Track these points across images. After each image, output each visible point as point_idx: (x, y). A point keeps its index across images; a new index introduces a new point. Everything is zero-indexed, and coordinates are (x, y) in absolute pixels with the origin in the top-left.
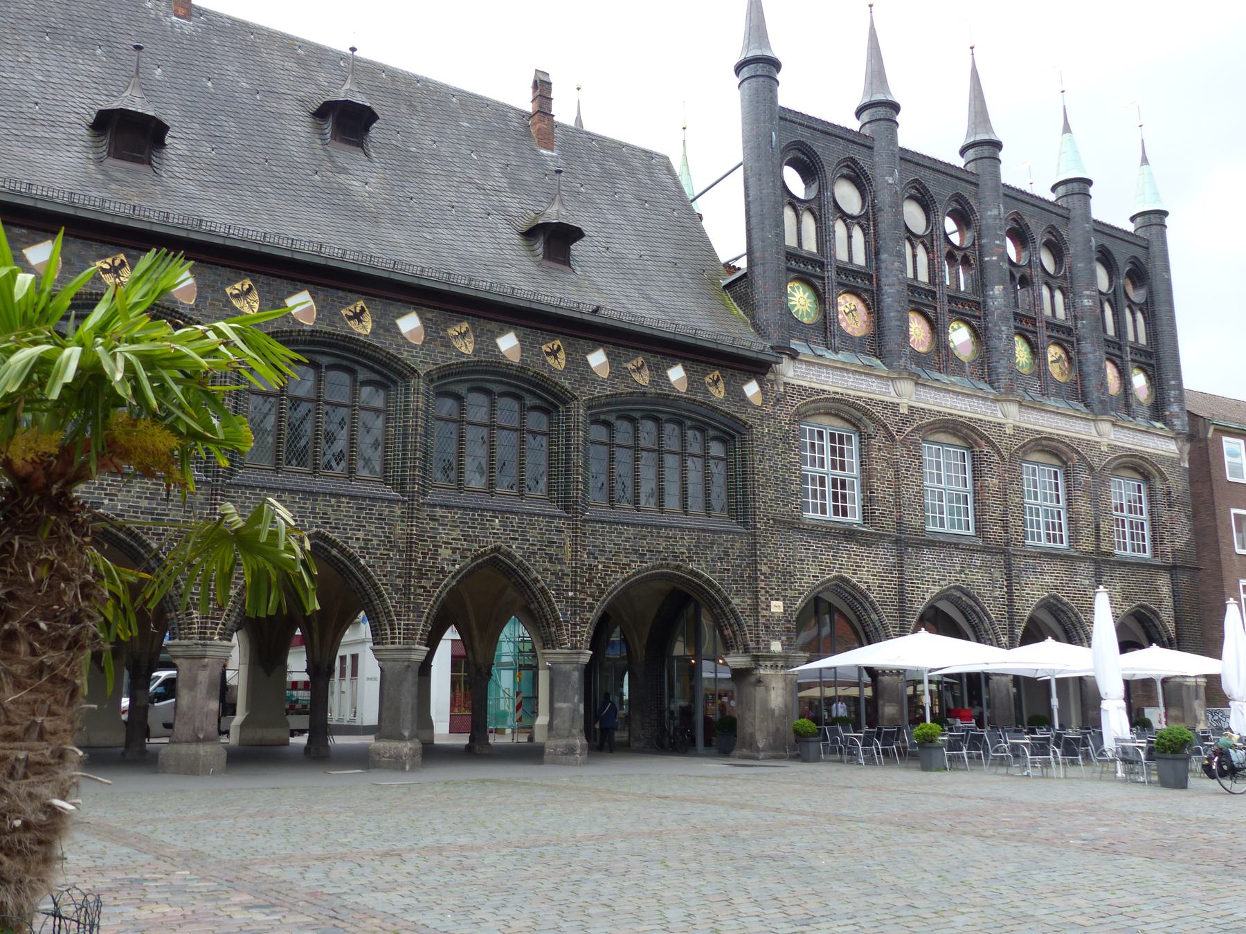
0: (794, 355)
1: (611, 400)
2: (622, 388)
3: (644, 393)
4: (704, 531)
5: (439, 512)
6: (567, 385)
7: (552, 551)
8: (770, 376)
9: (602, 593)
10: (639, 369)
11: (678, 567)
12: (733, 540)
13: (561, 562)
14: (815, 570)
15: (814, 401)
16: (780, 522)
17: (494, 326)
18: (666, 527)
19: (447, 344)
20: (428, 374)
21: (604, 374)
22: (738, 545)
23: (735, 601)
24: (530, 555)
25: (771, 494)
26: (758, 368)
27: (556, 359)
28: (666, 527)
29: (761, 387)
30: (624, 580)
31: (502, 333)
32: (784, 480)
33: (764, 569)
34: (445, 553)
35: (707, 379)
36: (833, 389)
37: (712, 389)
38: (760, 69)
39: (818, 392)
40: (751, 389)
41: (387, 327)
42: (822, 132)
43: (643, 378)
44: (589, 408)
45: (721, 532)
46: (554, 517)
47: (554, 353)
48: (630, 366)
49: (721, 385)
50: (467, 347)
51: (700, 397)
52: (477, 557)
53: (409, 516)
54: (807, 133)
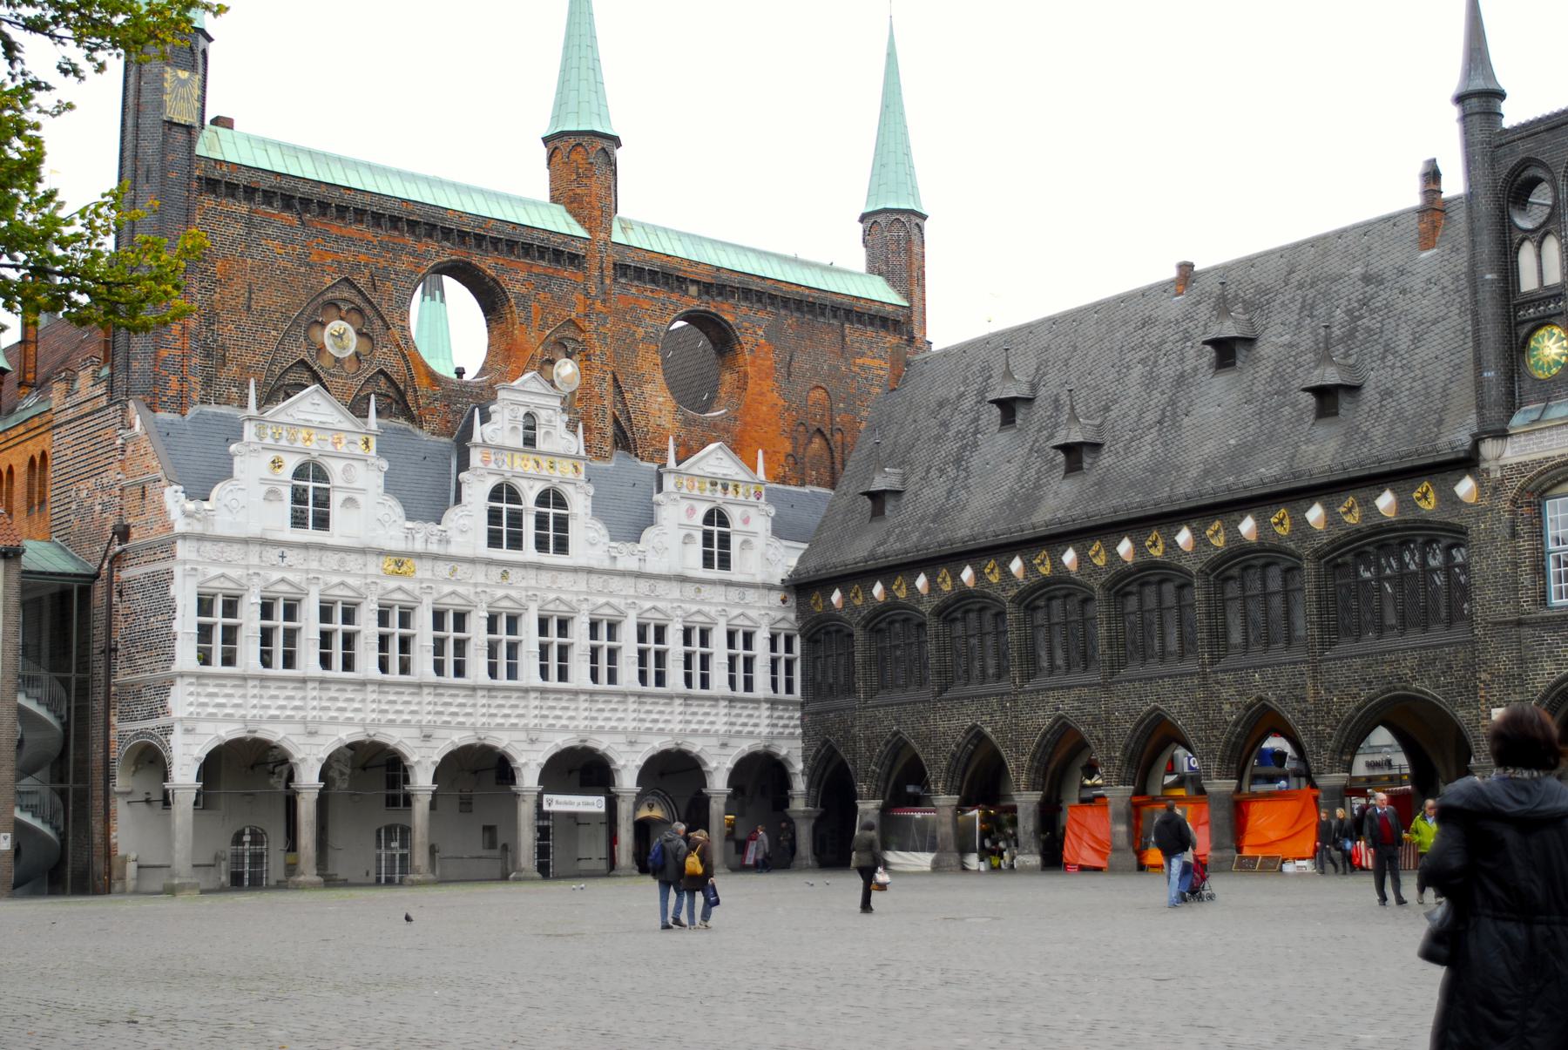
0: (1502, 434)
1: (1336, 546)
2: (1337, 533)
3: (1358, 531)
4: (1425, 648)
5: (1220, 676)
6: (1292, 545)
7: (1297, 692)
8: (1484, 465)
9: (1338, 721)
10: (1350, 510)
11: (1405, 688)
12: (1456, 652)
13: (1305, 700)
14: (1549, 666)
15: (1541, 473)
16: (1500, 623)
17: (1236, 516)
18: (1390, 652)
19: (1207, 544)
20: (1200, 571)
21: (1320, 527)
22: (1461, 656)
23: (1461, 713)
24: (1281, 699)
25: (1490, 594)
26: (1468, 463)
27: (1281, 522)
28: (1390, 652)
29: (1476, 480)
30: (1358, 709)
31: (1243, 518)
32: (1505, 575)
33: (1484, 676)
34: (1226, 707)
35: (1416, 495)
36: (1556, 453)
37: (1422, 504)
38: (1480, 101)
39: (1540, 463)
40: (1465, 488)
41: (1172, 546)
42: (1547, 130)
43: (1353, 519)
44: (1320, 558)
45: (1443, 645)
46: (1295, 663)
47: (1281, 523)
48: (1342, 509)
49: (1431, 495)
50: (1219, 542)
51: (1410, 516)
52: (1249, 707)
53: (1204, 685)
54: (1530, 144)
